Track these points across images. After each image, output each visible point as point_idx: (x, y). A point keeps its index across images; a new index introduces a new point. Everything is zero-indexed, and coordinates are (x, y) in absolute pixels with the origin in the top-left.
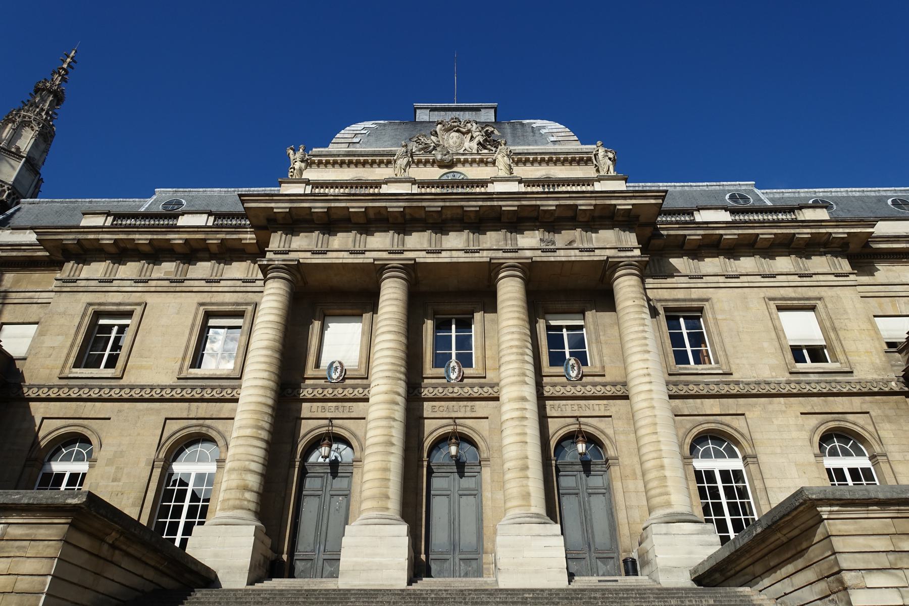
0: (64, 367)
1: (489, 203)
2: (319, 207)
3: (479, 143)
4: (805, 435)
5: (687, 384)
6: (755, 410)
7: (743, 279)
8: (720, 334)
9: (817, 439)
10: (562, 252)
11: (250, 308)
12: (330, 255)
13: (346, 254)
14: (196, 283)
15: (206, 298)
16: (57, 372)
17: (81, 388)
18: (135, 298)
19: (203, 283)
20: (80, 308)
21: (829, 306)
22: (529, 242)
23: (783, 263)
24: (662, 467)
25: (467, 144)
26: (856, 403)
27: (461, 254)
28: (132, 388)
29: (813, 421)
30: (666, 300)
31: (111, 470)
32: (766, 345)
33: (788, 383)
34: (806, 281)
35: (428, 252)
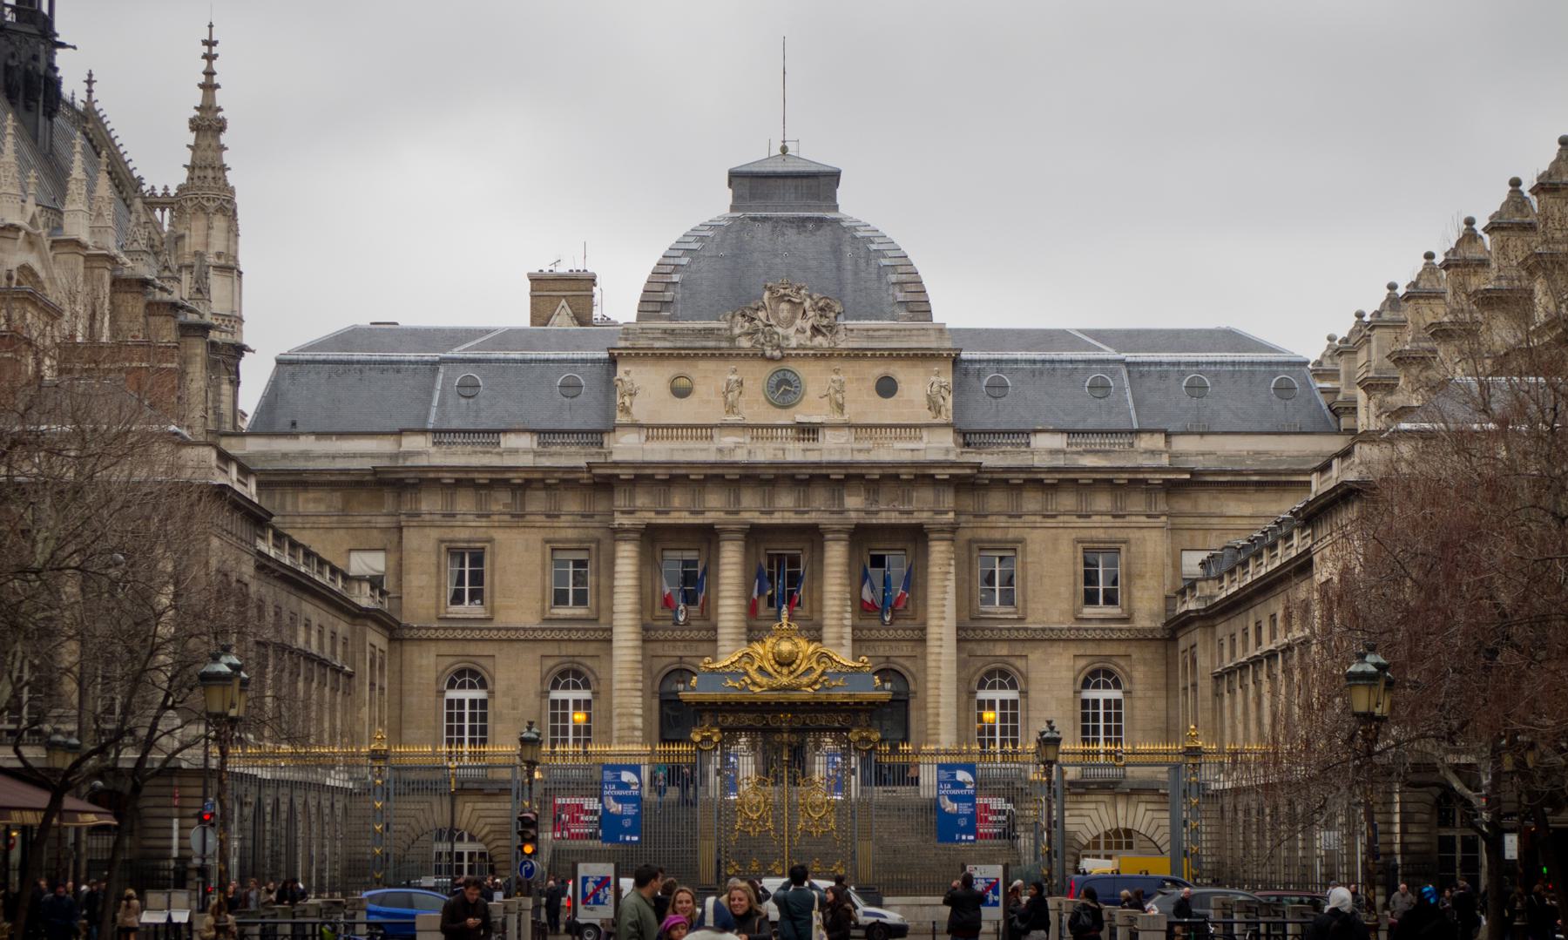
0: (438, 608)
1: (818, 472)
2: (661, 474)
3: (813, 327)
4: (1071, 675)
5: (983, 629)
6: (1035, 656)
7: (1061, 518)
8: (1024, 579)
9: (1081, 677)
10: (884, 515)
11: (593, 546)
12: (674, 515)
13: (686, 514)
14: (538, 518)
15: (550, 535)
16: (433, 611)
17: (463, 629)
18: (481, 534)
19: (543, 518)
20: (430, 545)
21: (1133, 549)
22: (854, 502)
23: (1102, 502)
24: (938, 715)
25: (799, 322)
26: (1120, 649)
27: (792, 515)
28: (508, 629)
29: (1082, 663)
30: (982, 541)
31: (509, 700)
32: (1063, 589)
33: (1069, 629)
34: (1119, 522)
35: (762, 512)
